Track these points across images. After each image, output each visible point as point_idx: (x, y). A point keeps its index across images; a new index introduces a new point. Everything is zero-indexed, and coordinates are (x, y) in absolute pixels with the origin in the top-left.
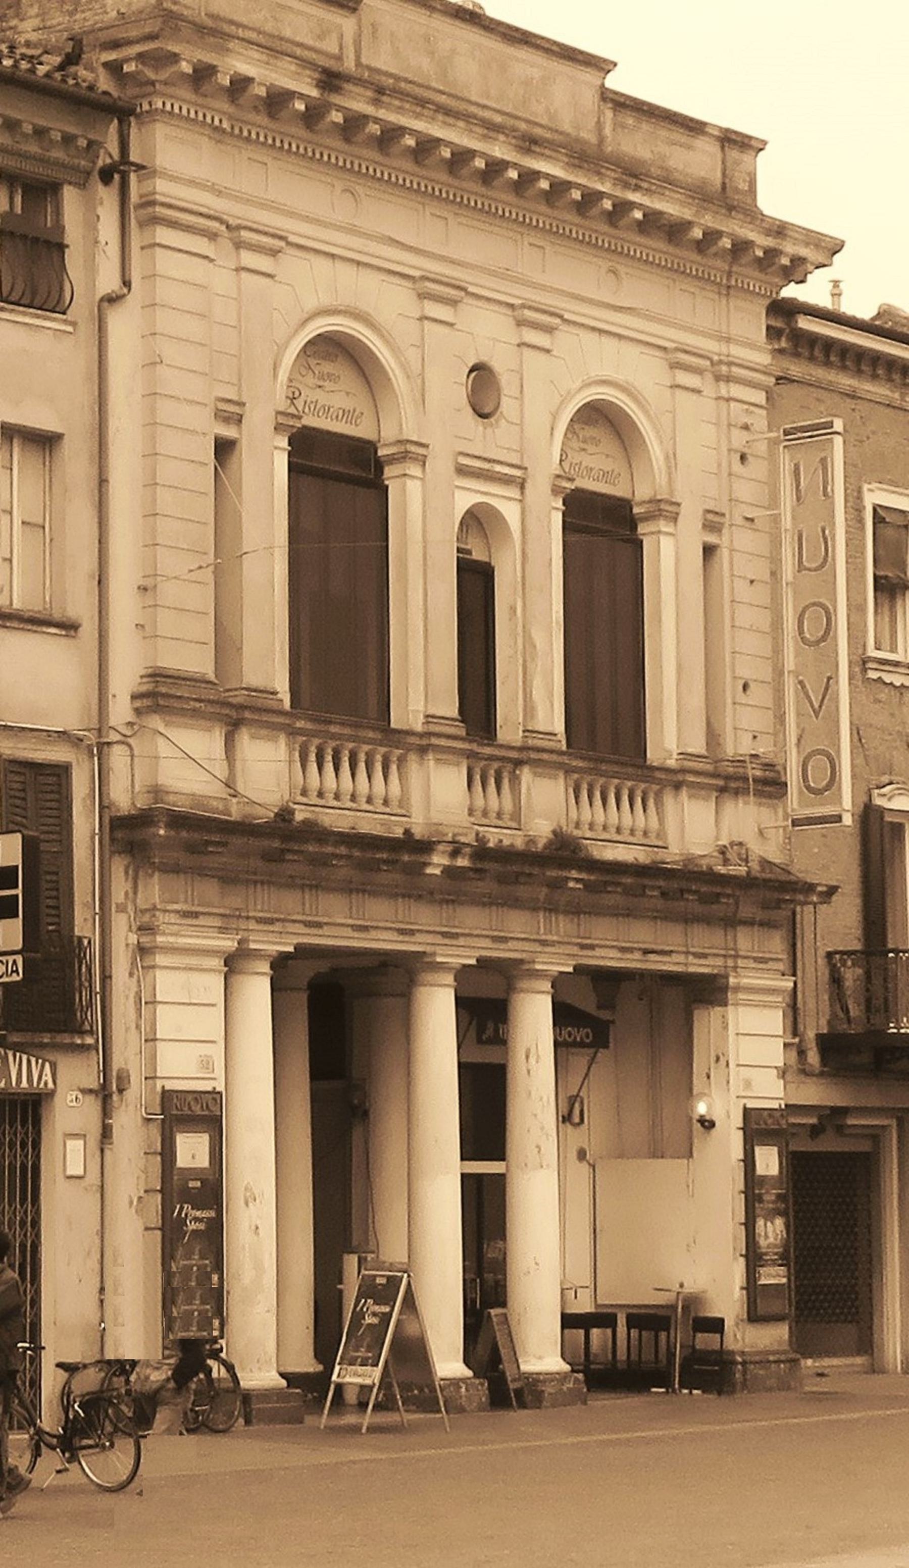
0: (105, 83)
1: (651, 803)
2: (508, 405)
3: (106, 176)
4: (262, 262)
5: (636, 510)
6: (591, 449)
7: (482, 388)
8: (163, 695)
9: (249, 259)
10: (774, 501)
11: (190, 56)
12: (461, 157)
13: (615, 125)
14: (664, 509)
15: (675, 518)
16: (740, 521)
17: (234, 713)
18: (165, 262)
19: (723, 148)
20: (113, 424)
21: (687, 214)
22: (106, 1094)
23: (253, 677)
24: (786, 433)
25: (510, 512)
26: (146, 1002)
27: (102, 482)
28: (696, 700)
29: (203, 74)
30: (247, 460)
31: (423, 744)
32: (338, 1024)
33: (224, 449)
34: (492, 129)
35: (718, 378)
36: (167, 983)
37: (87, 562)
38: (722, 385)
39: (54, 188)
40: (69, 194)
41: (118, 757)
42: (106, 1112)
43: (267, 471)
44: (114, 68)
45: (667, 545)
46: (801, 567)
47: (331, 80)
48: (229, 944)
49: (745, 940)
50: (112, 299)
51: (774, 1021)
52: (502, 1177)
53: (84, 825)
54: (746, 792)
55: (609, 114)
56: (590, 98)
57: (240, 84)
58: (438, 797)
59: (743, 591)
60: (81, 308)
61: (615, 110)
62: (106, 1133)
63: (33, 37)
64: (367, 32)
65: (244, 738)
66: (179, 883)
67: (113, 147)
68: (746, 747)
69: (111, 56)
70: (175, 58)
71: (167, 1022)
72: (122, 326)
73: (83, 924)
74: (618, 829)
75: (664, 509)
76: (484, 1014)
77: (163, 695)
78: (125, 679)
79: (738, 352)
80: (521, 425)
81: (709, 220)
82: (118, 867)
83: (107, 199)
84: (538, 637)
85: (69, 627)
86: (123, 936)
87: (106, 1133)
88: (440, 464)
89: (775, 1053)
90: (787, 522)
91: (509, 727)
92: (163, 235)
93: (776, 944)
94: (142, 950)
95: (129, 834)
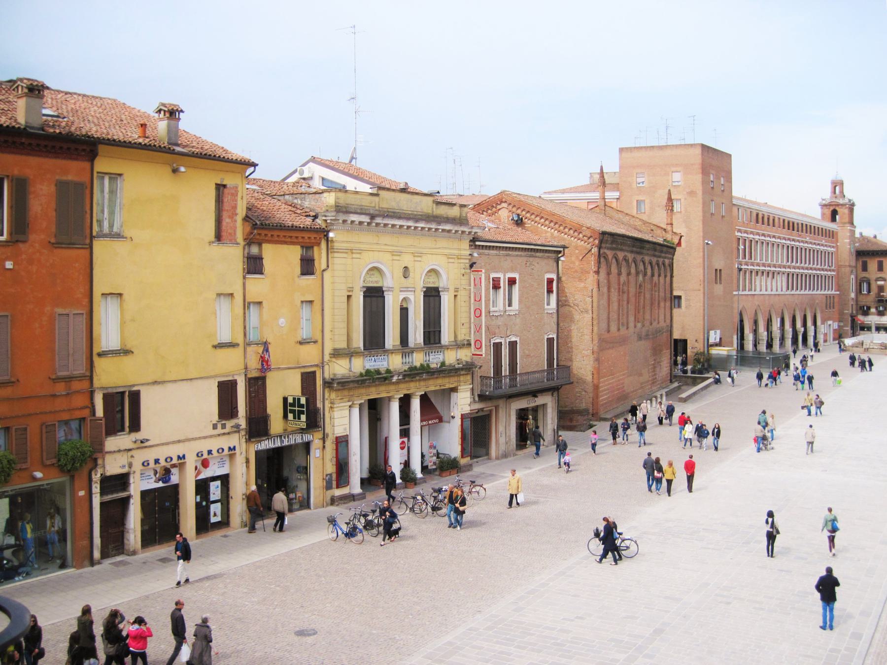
4: (358, 256)
8: (337, 354)
9: (354, 256)
10: (470, 285)
12: (401, 226)
14: (446, 289)
18: (337, 261)
22: (324, 440)
25: (412, 297)
27: (323, 310)
29: (344, 221)
30: (353, 299)
31: (392, 352)
32: (374, 411)
36: (337, 414)
40: (316, 248)
41: (326, 367)
42: (324, 443)
43: (359, 300)
44: (326, 221)
47: (373, 217)
48: (350, 403)
49: (462, 378)
50: (324, 270)
51: (468, 394)
53: (319, 382)
57: (352, 222)
58: (396, 362)
59: (463, 304)
62: (324, 447)
65: (353, 359)
66: (339, 393)
72: (327, 275)
73: (319, 405)
74: (435, 360)
75: (446, 289)
76: (405, 403)
77: (337, 354)
78: (328, 350)
82: (326, 391)
86: (327, 405)
87: (324, 447)
89: (468, 401)
90: (472, 290)
91: (411, 344)
92: (336, 255)
93: (469, 377)
94: (331, 407)
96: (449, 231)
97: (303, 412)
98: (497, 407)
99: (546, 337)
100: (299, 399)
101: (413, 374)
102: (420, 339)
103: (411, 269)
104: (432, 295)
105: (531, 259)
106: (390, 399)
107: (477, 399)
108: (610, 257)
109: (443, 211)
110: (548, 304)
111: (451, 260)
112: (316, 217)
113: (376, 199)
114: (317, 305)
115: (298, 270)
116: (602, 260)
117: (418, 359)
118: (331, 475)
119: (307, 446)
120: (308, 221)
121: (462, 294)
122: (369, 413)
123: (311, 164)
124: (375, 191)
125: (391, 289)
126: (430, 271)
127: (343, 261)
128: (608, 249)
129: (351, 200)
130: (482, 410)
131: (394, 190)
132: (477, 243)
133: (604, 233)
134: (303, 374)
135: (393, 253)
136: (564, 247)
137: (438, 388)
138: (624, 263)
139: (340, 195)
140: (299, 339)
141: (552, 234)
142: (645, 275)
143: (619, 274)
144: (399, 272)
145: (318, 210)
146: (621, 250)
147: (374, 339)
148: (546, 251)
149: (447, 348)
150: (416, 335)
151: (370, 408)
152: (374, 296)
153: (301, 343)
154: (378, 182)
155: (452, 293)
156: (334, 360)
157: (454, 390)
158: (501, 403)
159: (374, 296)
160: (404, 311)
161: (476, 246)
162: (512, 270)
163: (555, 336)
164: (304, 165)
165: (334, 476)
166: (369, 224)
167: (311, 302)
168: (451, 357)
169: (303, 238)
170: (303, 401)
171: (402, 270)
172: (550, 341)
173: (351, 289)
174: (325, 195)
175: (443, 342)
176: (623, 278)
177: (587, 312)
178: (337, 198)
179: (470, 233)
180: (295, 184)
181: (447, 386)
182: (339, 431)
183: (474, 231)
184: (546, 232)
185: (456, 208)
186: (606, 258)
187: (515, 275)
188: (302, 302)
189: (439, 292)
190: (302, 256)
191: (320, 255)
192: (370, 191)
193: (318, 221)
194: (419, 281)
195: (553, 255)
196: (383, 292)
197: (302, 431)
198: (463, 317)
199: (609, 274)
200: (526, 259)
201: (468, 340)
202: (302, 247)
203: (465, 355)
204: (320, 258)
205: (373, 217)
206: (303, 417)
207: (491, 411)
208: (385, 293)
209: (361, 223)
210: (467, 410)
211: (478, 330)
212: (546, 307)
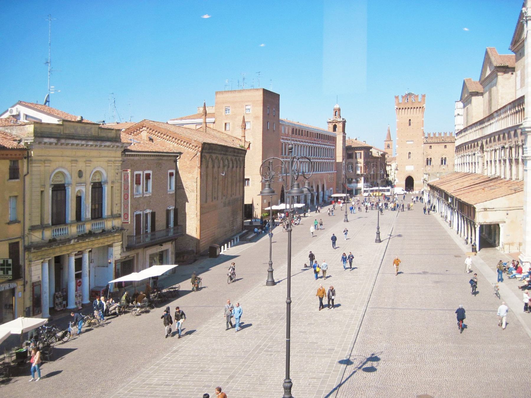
2: (84, 175)
3: (25, 158)
7: (80, 174)
8: (33, 228)
10: (121, 180)
17: (42, 227)
22: (24, 285)
23: (46, 223)
26: (30, 271)
27: (24, 201)
28: (110, 208)
30: (45, 193)
33: (42, 192)
36: (33, 268)
39: (17, 161)
40: (20, 161)
41: (26, 239)
42: (24, 288)
44: (27, 143)
48: (42, 260)
49: (116, 238)
50: (25, 175)
51: (120, 248)
52: (81, 273)
53: (21, 249)
56: (97, 129)
57: (45, 143)
60: (21, 176)
62: (24, 290)
71: (33, 273)
72: (27, 178)
73: (21, 263)
77: (33, 228)
78: (27, 226)
79: (117, 159)
83: (26, 161)
84: (87, 206)
85: (19, 222)
86: (27, 262)
87: (24, 290)
92: (34, 165)
95: (27, 249)
97: (10, 269)
98: (138, 254)
100: (7, 261)
101: (82, 237)
104: (97, 188)
105: (160, 161)
106: (69, 255)
107: (125, 250)
110: (170, 188)
112: (20, 141)
113: (62, 127)
114: (20, 199)
115: (7, 176)
117: (88, 227)
118: (29, 308)
119: (13, 291)
120: (15, 144)
122: (55, 266)
123: (18, 106)
124: (61, 123)
125: (69, 184)
130: (128, 256)
131: (73, 122)
134: (10, 244)
136: (180, 153)
137: (100, 245)
139: (37, 125)
140: (8, 221)
144: (75, 175)
145: (22, 136)
147: (59, 219)
148: (169, 156)
150: (87, 213)
151: (55, 262)
152: (59, 189)
153: (9, 224)
154: (63, 117)
155: (110, 185)
156: (31, 233)
157: (111, 246)
158: (140, 251)
160: (79, 199)
161: (126, 155)
164: (13, 107)
165: (31, 309)
166: (56, 144)
167: (16, 197)
168: (109, 224)
170: (10, 261)
173: (44, 186)
174: (27, 126)
175: (103, 216)
178: (35, 128)
179: (122, 147)
180: (6, 120)
181: (106, 244)
182: (35, 279)
184: (170, 144)
185: (114, 131)
188: (10, 197)
190: (10, 166)
191: (23, 166)
192: (58, 123)
193: (22, 143)
194: (88, 178)
196: (65, 187)
197: (9, 281)
198: (117, 200)
202: (11, 161)
203: (117, 223)
206: (10, 272)
207: (134, 257)
209: (51, 144)
210: (118, 257)
212: (168, 190)
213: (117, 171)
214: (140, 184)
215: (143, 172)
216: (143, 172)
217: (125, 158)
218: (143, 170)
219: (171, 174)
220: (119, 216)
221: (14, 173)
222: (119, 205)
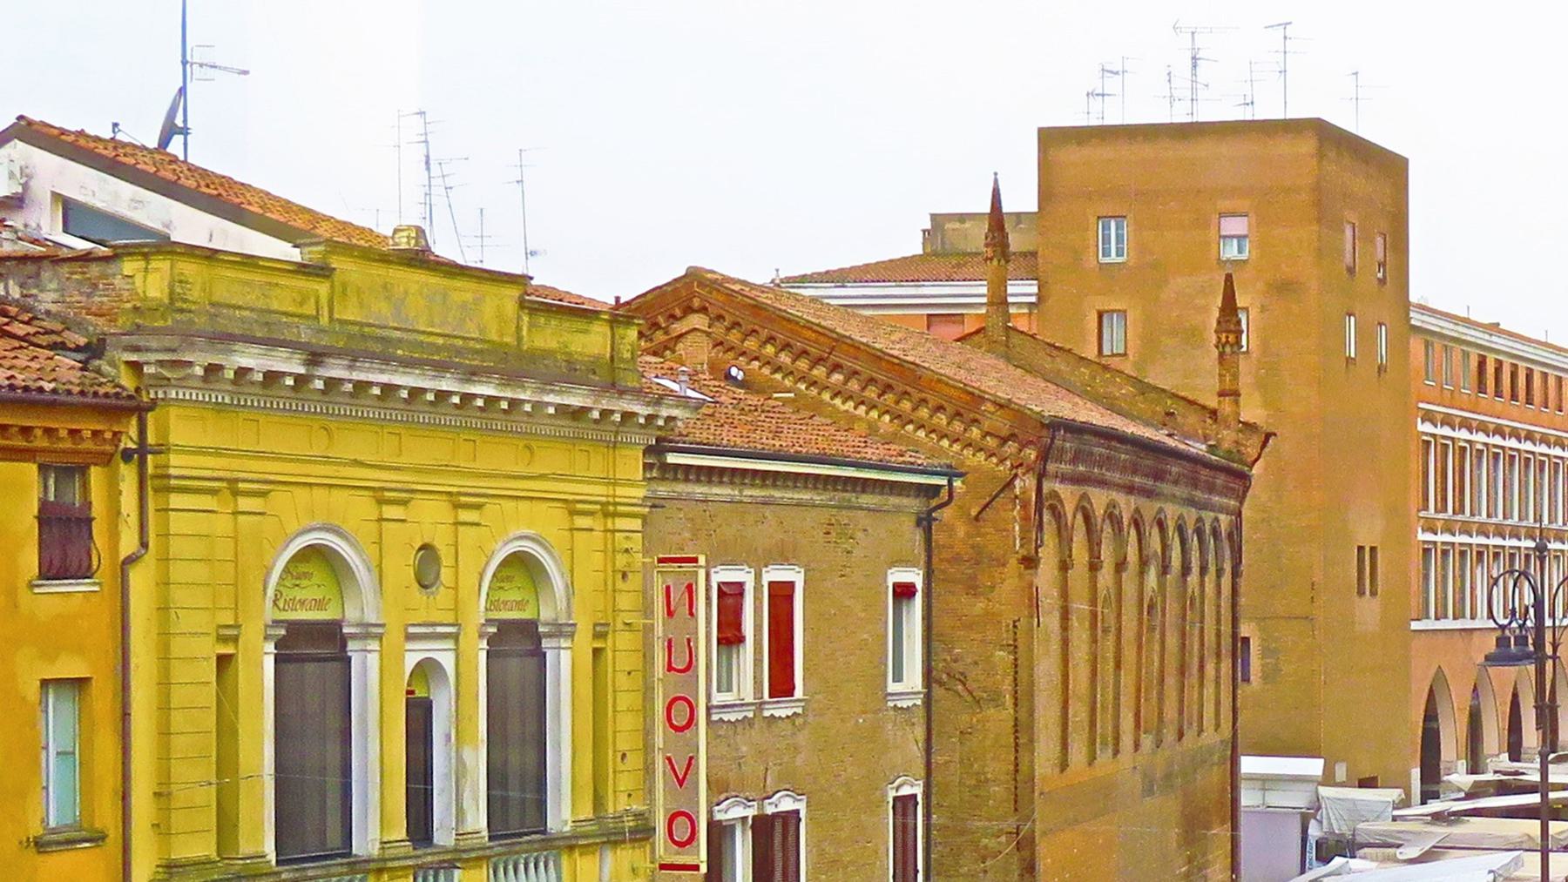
0: (128, 381)
1: (551, 864)
2: (446, 575)
3: (127, 455)
5: (541, 629)
6: (506, 585)
9: (245, 503)
10: (647, 611)
11: (200, 360)
12: (416, 393)
13: (531, 325)
15: (572, 635)
16: (620, 626)
19: (612, 328)
20: (134, 661)
21: (588, 403)
23: (245, 848)
24: (661, 561)
25: (447, 661)
27: (125, 715)
29: (213, 370)
30: (242, 668)
34: (441, 368)
35: (606, 515)
37: (108, 781)
38: (609, 521)
39: (83, 470)
40: (95, 473)
44: (136, 367)
45: (566, 656)
46: (670, 668)
47: (315, 358)
50: (131, 560)
54: (624, 842)
55: (526, 318)
56: (511, 307)
57: (242, 372)
59: (623, 681)
61: (530, 315)
63: (54, 308)
64: (338, 289)
67: (133, 431)
68: (623, 804)
69: (134, 357)
70: (190, 364)
72: (141, 580)
80: (456, 588)
81: (605, 404)
85: (98, 839)
88: (394, 635)
90: (659, 630)
91: (443, 836)
92: (176, 501)
96: (579, 413)
99: (892, 794)
102: (478, 819)
103: (446, 559)
105: (844, 517)
108: (1069, 508)
109: (548, 337)
110: (898, 678)
111: (582, 522)
113: (322, 288)
114: (102, 697)
116: (1047, 517)
121: (623, 643)
126: (506, 563)
127: (200, 523)
128: (1064, 479)
129: (228, 286)
132: (672, 458)
133: (1058, 425)
135: (380, 497)
138: (1108, 530)
140: (36, 830)
141: (873, 428)
142: (1165, 569)
143: (1094, 567)
144: (402, 568)
146: (1102, 483)
149: (570, 844)
152: (314, 651)
159: (314, 651)
160: (419, 716)
161: (665, 467)
162: (783, 557)
163: (918, 790)
167: (80, 683)
169: (48, 431)
171: (411, 557)
172: (904, 805)
175: (552, 824)
176: (1106, 577)
177: (995, 699)
178: (177, 281)
179: (650, 418)
183: (665, 413)
186: (1058, 515)
187: (794, 575)
188: (45, 683)
189: (538, 638)
195: (914, 504)
199: (1064, 566)
200: (824, 516)
201: (638, 816)
202: (43, 469)
204: (115, 512)
205: (315, 358)
208: (351, 645)
209: (272, 377)
211: (682, 777)
212: (893, 687)
213: (621, 561)
214: (741, 640)
215: (758, 577)
216: (758, 577)
217: (663, 490)
218: (759, 562)
219: (904, 592)
220: (642, 833)
221: (65, 542)
222: (635, 761)
